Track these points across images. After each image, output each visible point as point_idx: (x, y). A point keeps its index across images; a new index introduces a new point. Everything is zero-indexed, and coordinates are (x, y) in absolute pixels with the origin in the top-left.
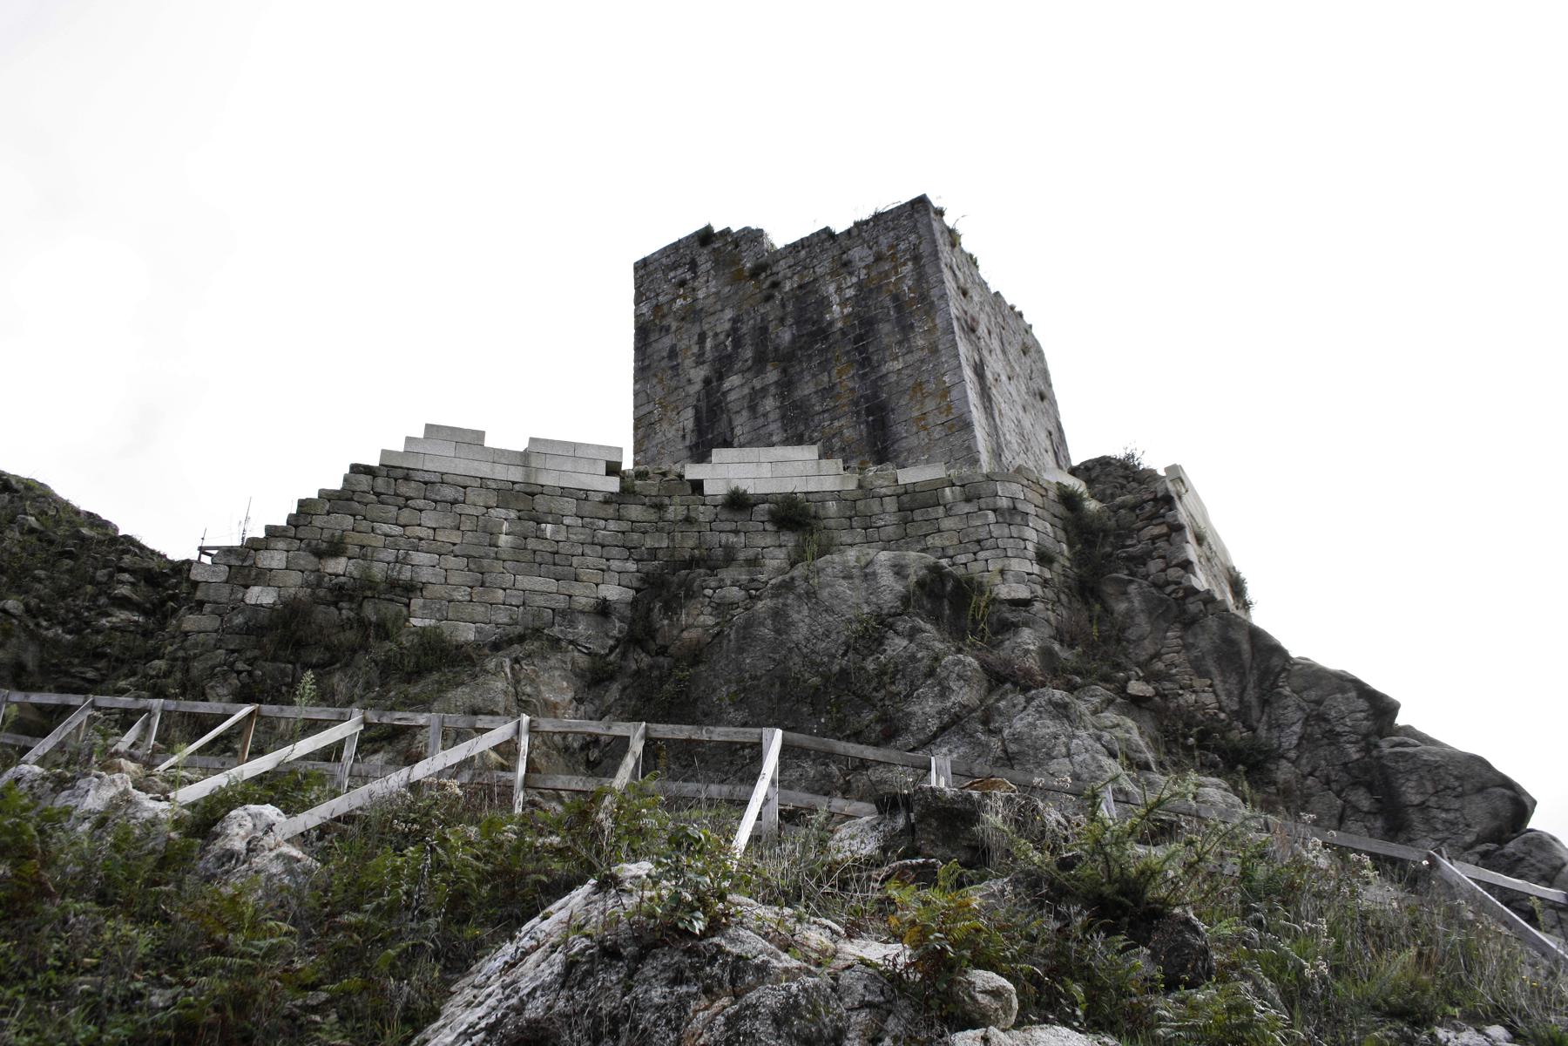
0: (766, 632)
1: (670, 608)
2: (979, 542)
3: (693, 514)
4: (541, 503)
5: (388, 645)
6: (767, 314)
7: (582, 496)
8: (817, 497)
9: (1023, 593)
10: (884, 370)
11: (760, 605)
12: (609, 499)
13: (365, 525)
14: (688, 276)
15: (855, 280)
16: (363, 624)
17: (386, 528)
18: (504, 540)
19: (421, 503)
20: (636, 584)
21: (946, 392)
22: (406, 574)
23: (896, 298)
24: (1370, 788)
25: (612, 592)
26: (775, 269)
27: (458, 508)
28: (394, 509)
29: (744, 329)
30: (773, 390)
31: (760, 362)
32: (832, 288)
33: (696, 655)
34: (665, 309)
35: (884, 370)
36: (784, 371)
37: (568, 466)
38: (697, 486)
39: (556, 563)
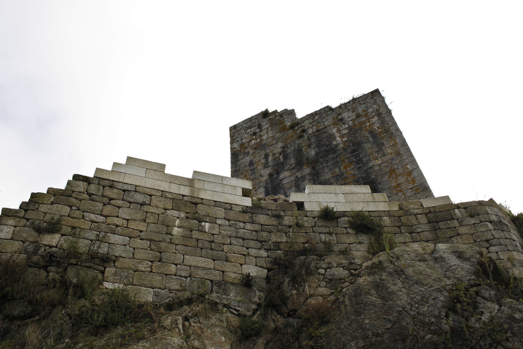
0: (373, 298)
1: (296, 281)
2: (487, 241)
3: (300, 222)
5: (83, 302)
6: (301, 143)
7: (229, 207)
8: (376, 214)
10: (371, 165)
11: (361, 280)
12: (245, 210)
13: (78, 213)
14: (257, 130)
15: (346, 126)
16: (65, 284)
17: (93, 217)
18: (176, 231)
19: (120, 203)
20: (269, 266)
21: (410, 173)
22: (104, 249)
23: (371, 132)
25: (252, 270)
26: (302, 125)
27: (145, 208)
28: (100, 205)
29: (289, 151)
30: (308, 177)
31: (299, 165)
32: (335, 130)
33: (322, 317)
34: (246, 145)
35: (371, 165)
36: (313, 168)
38: (300, 205)
39: (212, 248)
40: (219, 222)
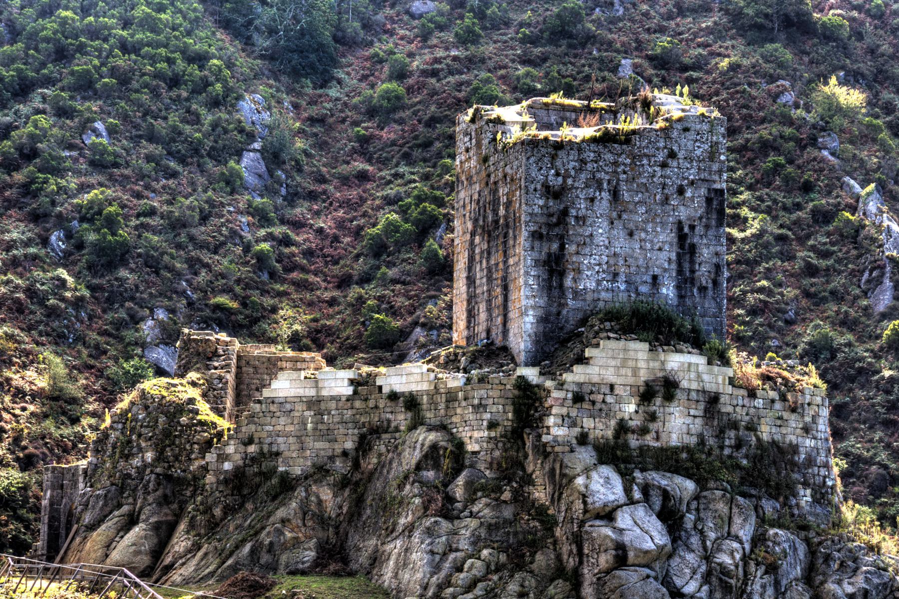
4: (323, 406)
7: (336, 399)
9: (476, 448)
12: (349, 399)
13: (259, 428)
18: (309, 426)
19: (278, 414)
22: (275, 449)
24: (576, 542)
25: (349, 445)
28: (269, 419)
37: (333, 385)
39: (327, 435)
40: (333, 412)
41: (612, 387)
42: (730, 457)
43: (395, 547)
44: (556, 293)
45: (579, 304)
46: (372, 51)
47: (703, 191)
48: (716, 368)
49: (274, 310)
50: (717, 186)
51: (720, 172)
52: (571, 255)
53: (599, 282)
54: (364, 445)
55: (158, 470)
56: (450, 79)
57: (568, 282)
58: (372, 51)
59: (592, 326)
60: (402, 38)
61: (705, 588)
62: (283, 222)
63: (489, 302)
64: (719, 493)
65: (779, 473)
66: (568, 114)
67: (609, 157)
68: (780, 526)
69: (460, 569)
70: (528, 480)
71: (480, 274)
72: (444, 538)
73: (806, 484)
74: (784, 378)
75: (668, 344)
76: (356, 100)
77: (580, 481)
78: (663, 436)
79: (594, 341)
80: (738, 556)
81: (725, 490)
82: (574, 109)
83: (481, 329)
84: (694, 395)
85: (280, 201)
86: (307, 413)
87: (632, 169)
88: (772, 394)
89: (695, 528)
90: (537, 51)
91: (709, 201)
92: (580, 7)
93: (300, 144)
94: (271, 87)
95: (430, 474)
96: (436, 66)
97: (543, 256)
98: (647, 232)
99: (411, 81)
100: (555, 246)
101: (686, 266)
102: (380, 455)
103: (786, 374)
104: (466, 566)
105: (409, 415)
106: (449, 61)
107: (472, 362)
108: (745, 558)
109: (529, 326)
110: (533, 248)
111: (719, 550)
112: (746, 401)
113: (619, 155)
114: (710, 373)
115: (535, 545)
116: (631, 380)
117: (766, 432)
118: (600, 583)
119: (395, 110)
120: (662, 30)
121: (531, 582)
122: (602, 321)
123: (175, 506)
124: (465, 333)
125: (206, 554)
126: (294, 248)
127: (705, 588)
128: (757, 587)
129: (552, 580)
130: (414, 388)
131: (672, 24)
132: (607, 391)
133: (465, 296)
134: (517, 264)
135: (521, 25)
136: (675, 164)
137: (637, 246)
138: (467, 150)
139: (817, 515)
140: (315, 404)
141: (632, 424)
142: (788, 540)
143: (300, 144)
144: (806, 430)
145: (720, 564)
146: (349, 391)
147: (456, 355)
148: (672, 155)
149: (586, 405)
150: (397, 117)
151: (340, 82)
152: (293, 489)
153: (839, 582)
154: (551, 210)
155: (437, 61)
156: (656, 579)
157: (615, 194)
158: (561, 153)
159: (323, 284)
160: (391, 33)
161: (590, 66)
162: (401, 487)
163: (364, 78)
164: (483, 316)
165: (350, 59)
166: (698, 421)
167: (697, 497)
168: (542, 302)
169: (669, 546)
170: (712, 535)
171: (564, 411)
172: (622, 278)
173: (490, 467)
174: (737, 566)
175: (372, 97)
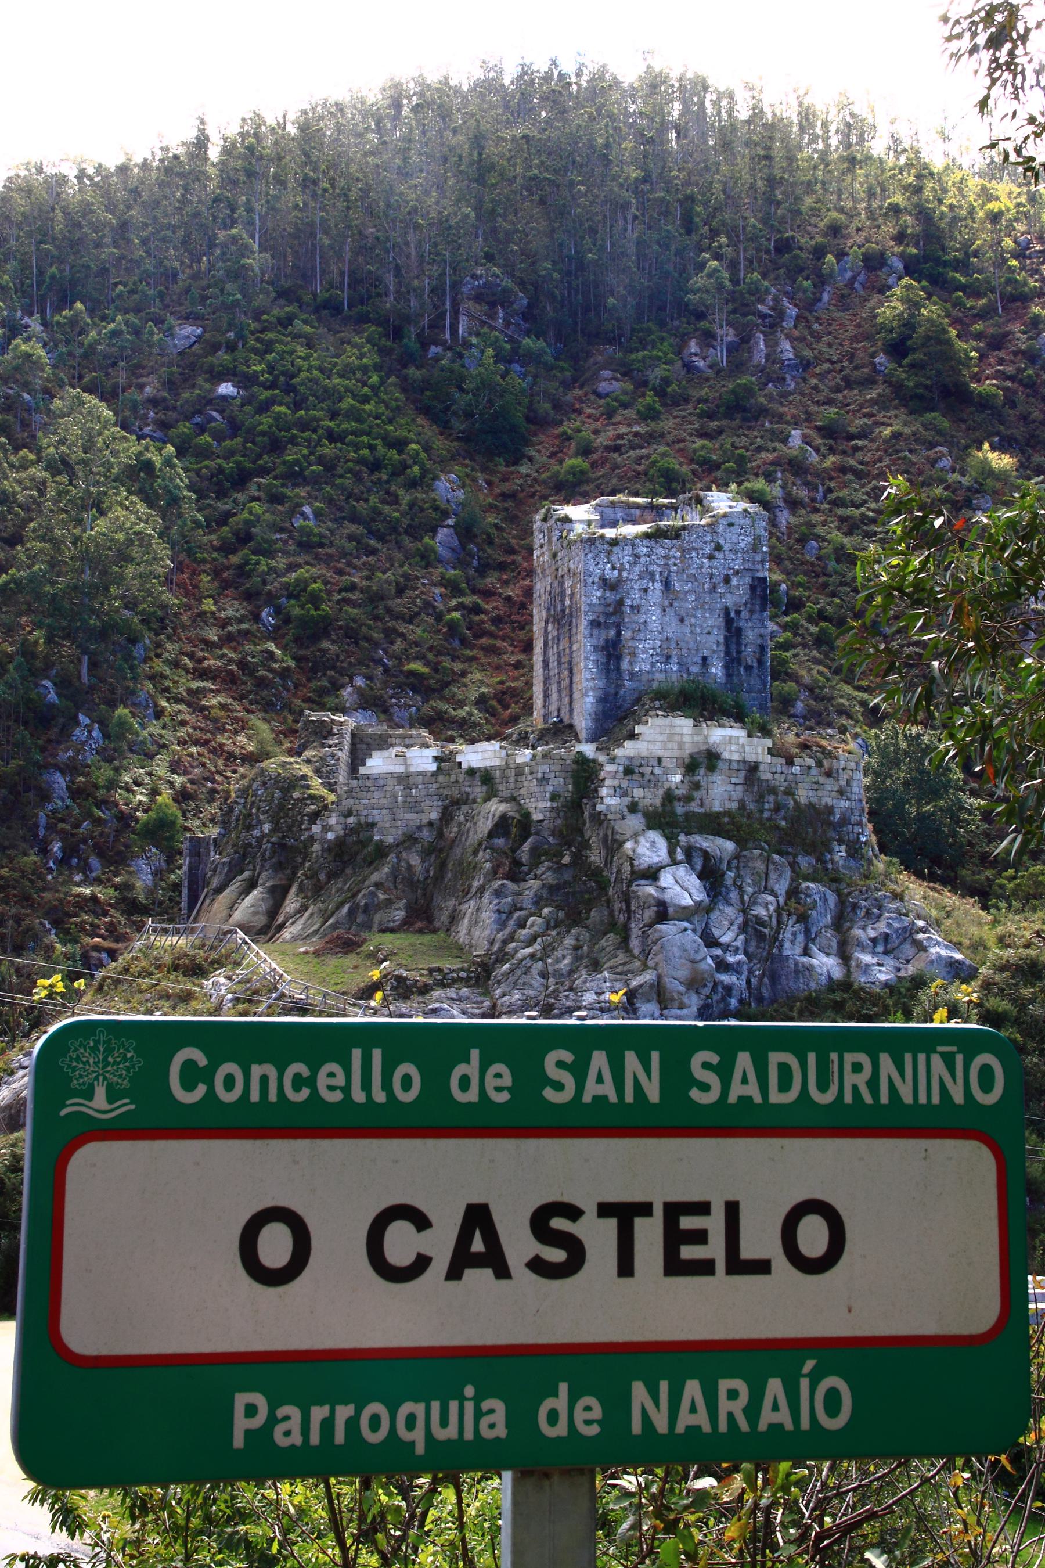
4: (411, 781)
9: (541, 817)
12: (434, 774)
22: (370, 820)
25: (434, 816)
39: (415, 806)
41: (659, 760)
42: (769, 819)
43: (469, 907)
44: (613, 675)
45: (635, 685)
46: (561, 430)
47: (748, 580)
48: (756, 740)
49: (464, 674)
50: (760, 575)
51: (763, 562)
52: (627, 640)
53: (653, 665)
54: (446, 816)
55: (273, 840)
56: (632, 453)
57: (625, 665)
58: (561, 430)
59: (644, 705)
60: (589, 417)
61: (742, 937)
62: (474, 591)
63: (559, 683)
64: (757, 852)
65: (815, 832)
66: (633, 511)
67: (661, 551)
68: (813, 881)
69: (522, 926)
70: (586, 845)
71: (553, 659)
72: (509, 899)
73: (840, 842)
74: (820, 747)
75: (712, 720)
76: (544, 476)
77: (629, 845)
78: (706, 802)
79: (644, 719)
80: (771, 908)
81: (762, 849)
82: (637, 506)
83: (553, 708)
84: (735, 765)
85: (472, 572)
86: (398, 788)
87: (682, 562)
88: (811, 762)
89: (735, 884)
90: (714, 424)
91: (753, 588)
92: (752, 383)
93: (491, 519)
94: (467, 466)
95: (500, 842)
96: (619, 442)
97: (602, 643)
98: (696, 617)
99: (594, 457)
100: (612, 633)
101: (733, 647)
102: (460, 824)
103: (824, 743)
104: (528, 923)
105: (485, 788)
106: (630, 437)
107: (539, 739)
108: (779, 910)
109: (589, 706)
110: (591, 635)
111: (755, 903)
112: (785, 769)
113: (670, 549)
114: (750, 744)
115: (589, 905)
116: (676, 753)
117: (804, 795)
118: (644, 936)
119: (580, 483)
120: (829, 402)
121: (585, 935)
122: (652, 700)
123: (289, 871)
124: (542, 712)
125: (312, 914)
126: (483, 616)
127: (742, 937)
128: (788, 935)
129: (605, 934)
130: (488, 763)
131: (840, 396)
132: (655, 763)
133: (541, 678)
134: (579, 649)
135: (699, 401)
136: (721, 555)
137: (688, 630)
138: (542, 546)
139: (850, 868)
140: (405, 779)
141: (678, 792)
142: (819, 892)
143: (491, 519)
144: (841, 792)
145: (756, 916)
146: (433, 767)
147: (526, 733)
148: (718, 548)
149: (636, 777)
150: (581, 490)
151: (531, 459)
152: (387, 856)
153: (864, 928)
154: (608, 601)
155: (620, 437)
156: (694, 931)
157: (667, 584)
158: (615, 549)
159: (510, 649)
160: (579, 412)
161: (762, 437)
162: (475, 853)
163: (553, 455)
164: (555, 696)
165: (542, 437)
166: (740, 788)
167: (737, 857)
168: (601, 684)
169: (707, 900)
170: (750, 890)
171: (616, 783)
172: (675, 660)
173: (553, 834)
174: (770, 917)
175: (559, 472)
